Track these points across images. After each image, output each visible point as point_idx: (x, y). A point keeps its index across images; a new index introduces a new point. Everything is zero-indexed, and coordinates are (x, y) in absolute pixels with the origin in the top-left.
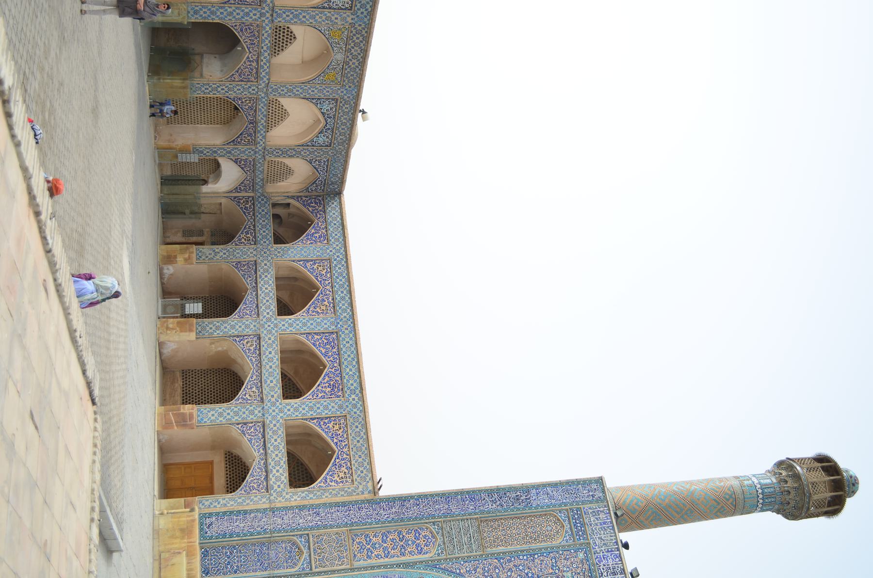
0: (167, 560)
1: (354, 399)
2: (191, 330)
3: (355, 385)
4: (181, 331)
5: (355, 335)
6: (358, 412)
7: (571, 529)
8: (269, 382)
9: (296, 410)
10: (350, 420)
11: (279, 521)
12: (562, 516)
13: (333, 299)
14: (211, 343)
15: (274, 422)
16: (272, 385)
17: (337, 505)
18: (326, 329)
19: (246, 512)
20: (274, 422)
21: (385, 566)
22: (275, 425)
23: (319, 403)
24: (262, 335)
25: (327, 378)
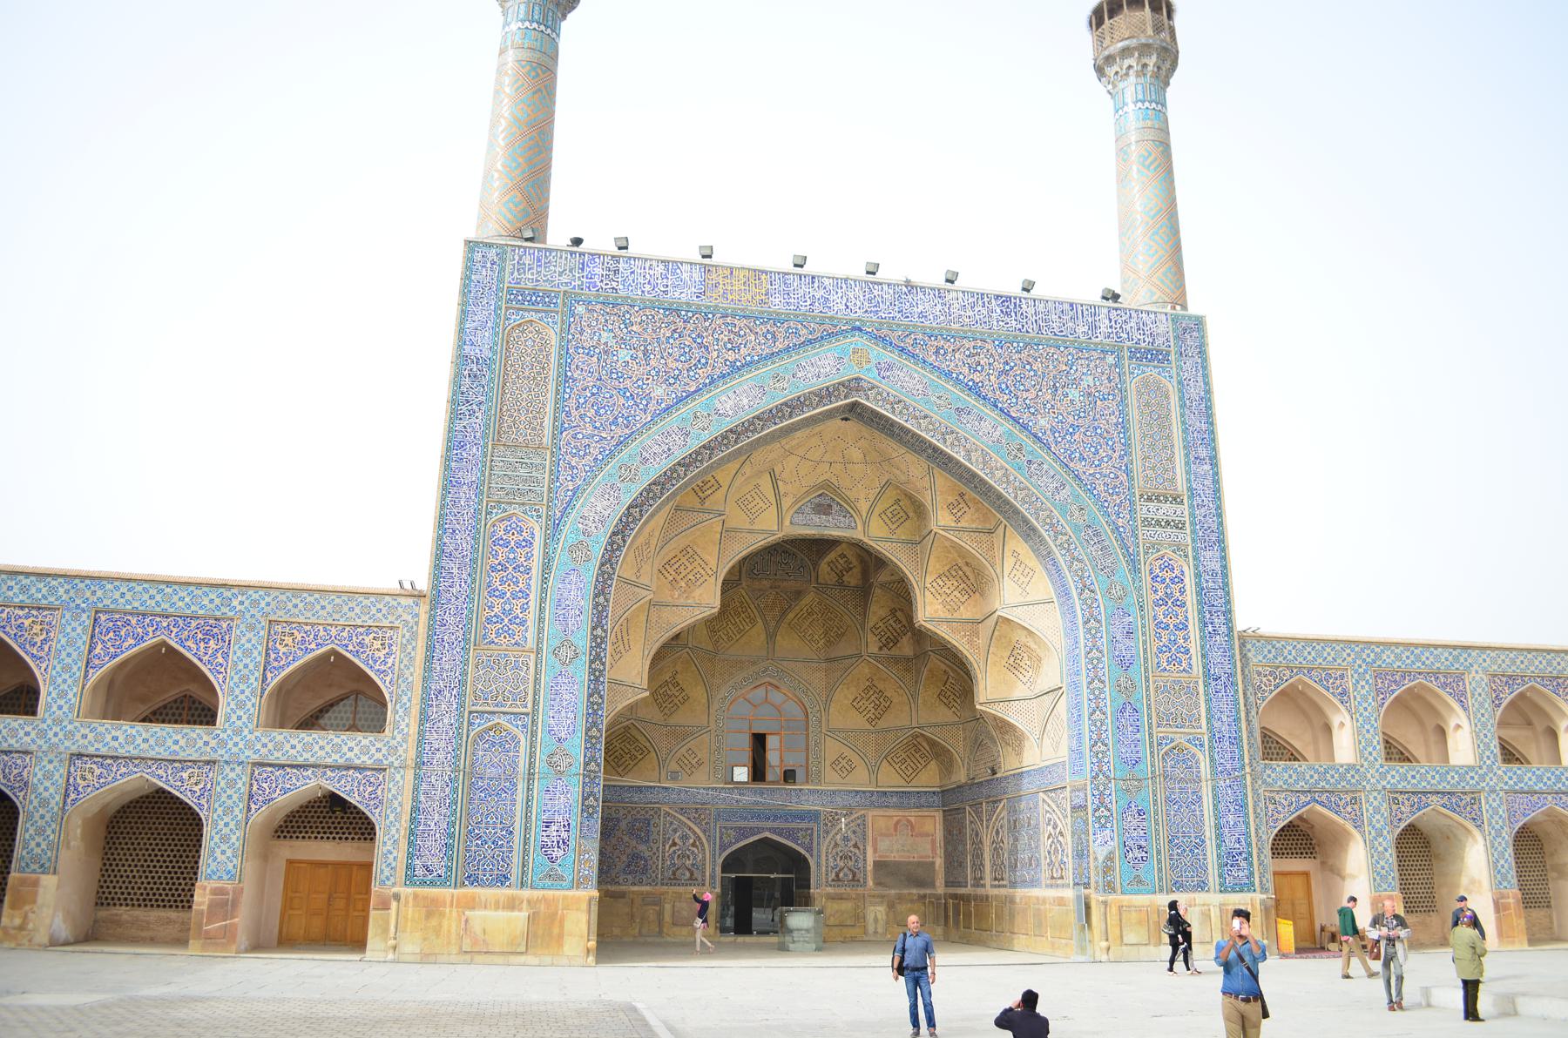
0: (475, 942)
1: (242, 603)
2: (36, 883)
3: (212, 596)
4: (34, 902)
5: (111, 579)
6: (268, 599)
7: (537, 311)
8: (176, 748)
9: (241, 705)
10: (281, 615)
11: (440, 756)
12: (515, 318)
13: (22, 608)
14: (68, 847)
15: (259, 746)
16: (182, 742)
17: (429, 659)
18: (84, 629)
19: (415, 809)
20: (259, 746)
21: (543, 601)
22: (265, 745)
23: (236, 664)
24: (74, 749)
25: (189, 643)
